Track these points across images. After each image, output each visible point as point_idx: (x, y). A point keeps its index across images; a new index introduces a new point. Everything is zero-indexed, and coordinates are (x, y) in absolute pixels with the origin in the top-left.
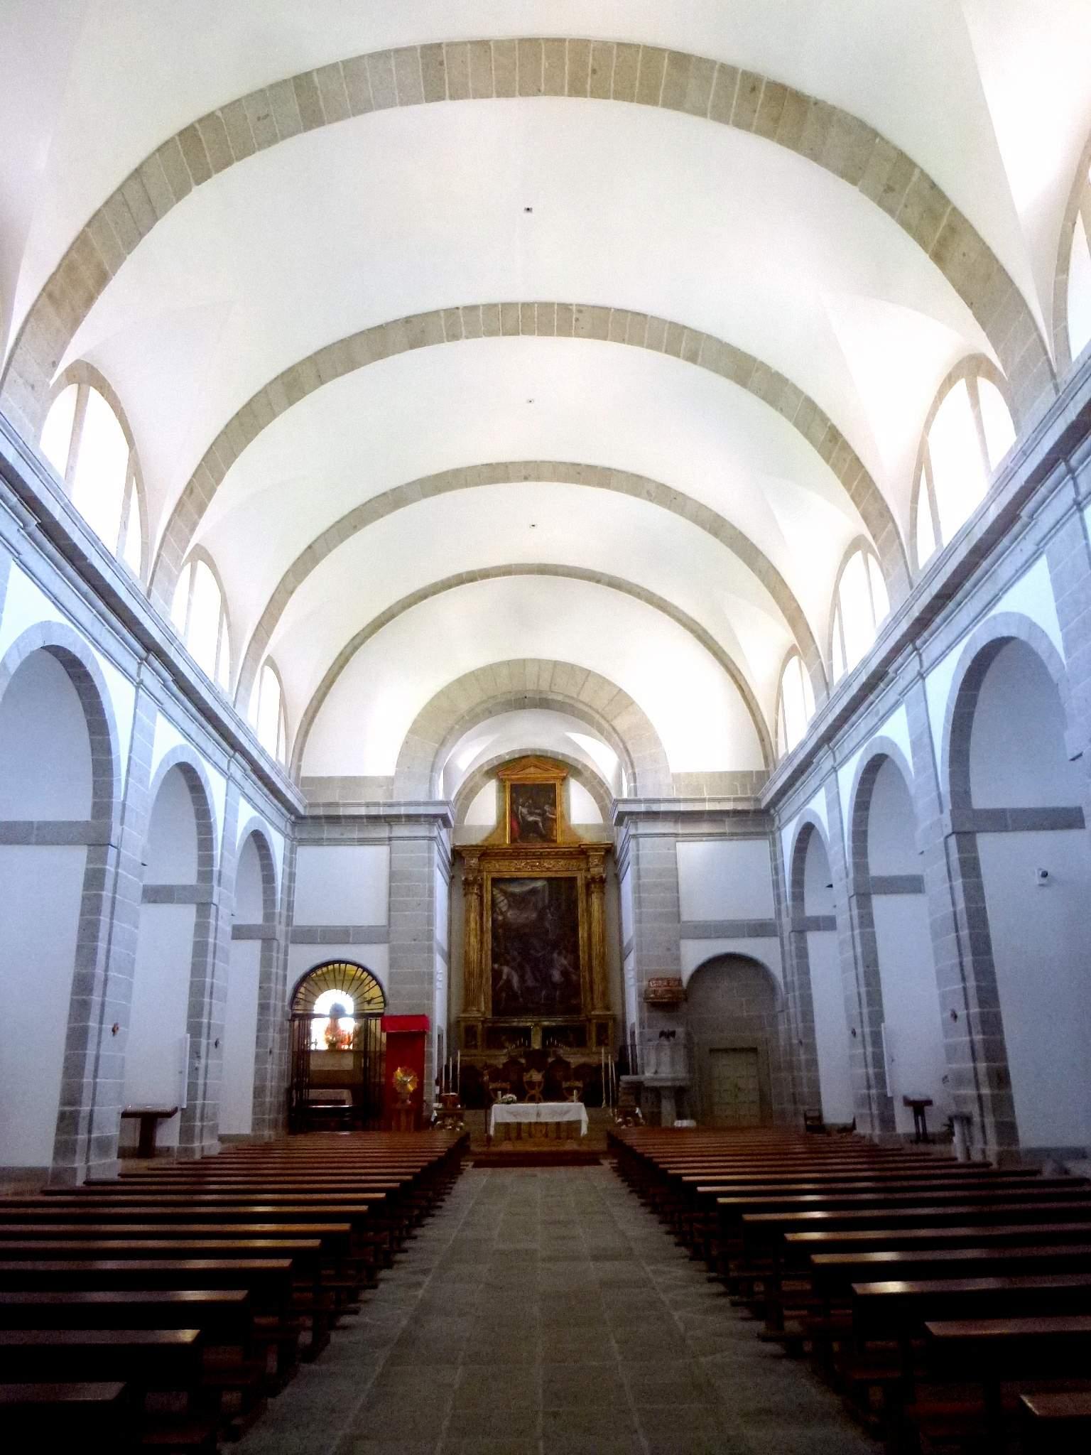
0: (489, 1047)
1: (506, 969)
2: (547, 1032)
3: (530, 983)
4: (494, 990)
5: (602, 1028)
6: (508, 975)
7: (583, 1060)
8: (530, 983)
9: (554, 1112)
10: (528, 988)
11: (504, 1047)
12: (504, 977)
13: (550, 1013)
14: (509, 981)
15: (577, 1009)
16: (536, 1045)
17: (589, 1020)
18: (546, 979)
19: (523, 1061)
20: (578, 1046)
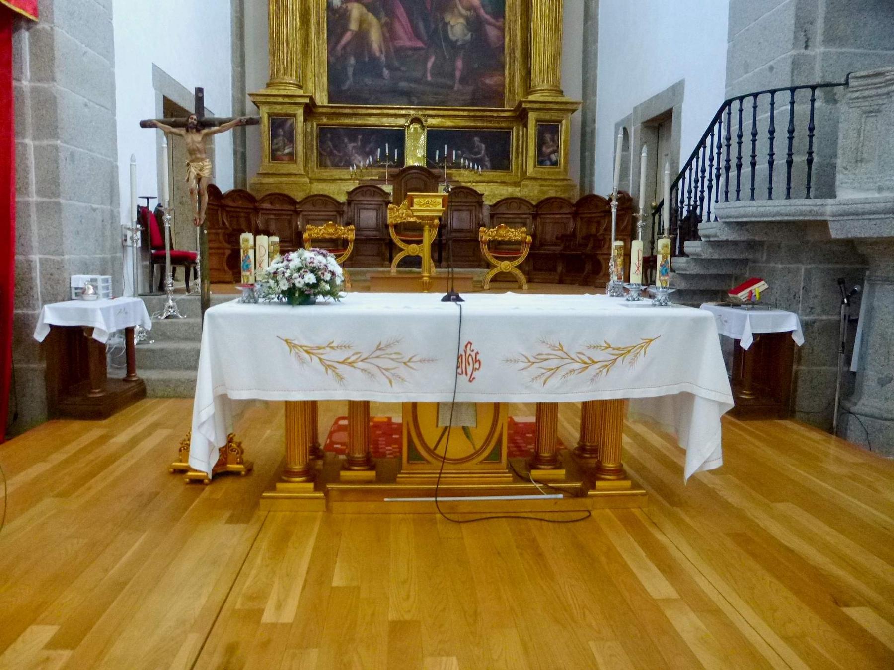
0: (322, 164)
1: (356, 10)
2: (435, 138)
3: (405, 40)
4: (331, 51)
5: (549, 130)
6: (361, 22)
7: (506, 191)
8: (405, 40)
9: (551, 352)
10: (399, 50)
11: (348, 164)
12: (353, 26)
13: (440, 99)
14: (362, 36)
15: (496, 96)
16: (416, 154)
17: (521, 115)
18: (437, 36)
19: (388, 188)
20: (494, 168)
